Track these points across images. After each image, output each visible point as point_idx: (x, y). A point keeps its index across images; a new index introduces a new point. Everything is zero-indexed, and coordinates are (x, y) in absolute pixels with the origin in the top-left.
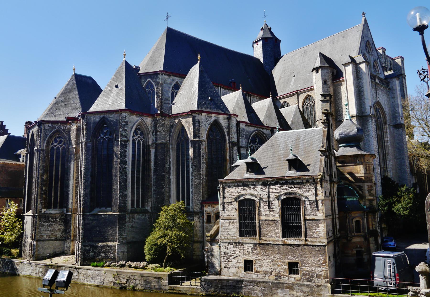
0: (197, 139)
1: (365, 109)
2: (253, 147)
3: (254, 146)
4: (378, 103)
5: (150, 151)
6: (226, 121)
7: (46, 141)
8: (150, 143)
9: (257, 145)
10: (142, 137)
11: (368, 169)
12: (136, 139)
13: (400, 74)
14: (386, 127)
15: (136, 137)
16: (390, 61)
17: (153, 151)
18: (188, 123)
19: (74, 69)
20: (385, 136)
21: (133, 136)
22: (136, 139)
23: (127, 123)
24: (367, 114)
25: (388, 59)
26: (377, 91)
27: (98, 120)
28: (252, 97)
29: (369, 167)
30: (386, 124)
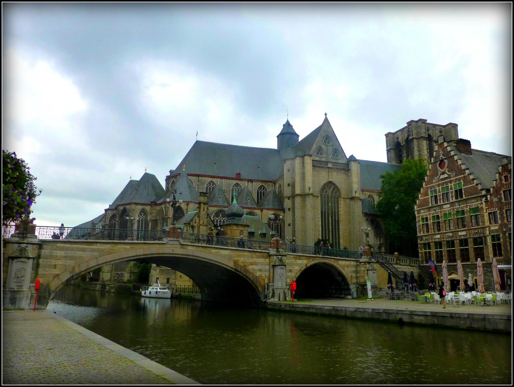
0: (167, 217)
1: (306, 189)
2: (217, 220)
3: (217, 218)
4: (330, 183)
5: (149, 224)
6: (186, 205)
7: (108, 220)
8: (149, 220)
9: (220, 218)
10: (144, 217)
11: (232, 232)
12: (141, 218)
13: (450, 140)
14: (341, 200)
15: (141, 216)
16: (440, 129)
17: (150, 224)
18: (164, 208)
19: (131, 178)
20: (339, 207)
21: (139, 216)
22: (141, 218)
23: (133, 210)
24: (306, 193)
25: (437, 127)
26: (330, 174)
27: (123, 209)
28: (254, 182)
29: (233, 231)
30: (341, 197)
